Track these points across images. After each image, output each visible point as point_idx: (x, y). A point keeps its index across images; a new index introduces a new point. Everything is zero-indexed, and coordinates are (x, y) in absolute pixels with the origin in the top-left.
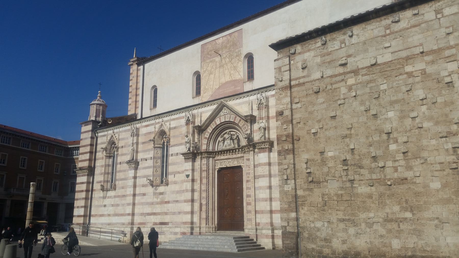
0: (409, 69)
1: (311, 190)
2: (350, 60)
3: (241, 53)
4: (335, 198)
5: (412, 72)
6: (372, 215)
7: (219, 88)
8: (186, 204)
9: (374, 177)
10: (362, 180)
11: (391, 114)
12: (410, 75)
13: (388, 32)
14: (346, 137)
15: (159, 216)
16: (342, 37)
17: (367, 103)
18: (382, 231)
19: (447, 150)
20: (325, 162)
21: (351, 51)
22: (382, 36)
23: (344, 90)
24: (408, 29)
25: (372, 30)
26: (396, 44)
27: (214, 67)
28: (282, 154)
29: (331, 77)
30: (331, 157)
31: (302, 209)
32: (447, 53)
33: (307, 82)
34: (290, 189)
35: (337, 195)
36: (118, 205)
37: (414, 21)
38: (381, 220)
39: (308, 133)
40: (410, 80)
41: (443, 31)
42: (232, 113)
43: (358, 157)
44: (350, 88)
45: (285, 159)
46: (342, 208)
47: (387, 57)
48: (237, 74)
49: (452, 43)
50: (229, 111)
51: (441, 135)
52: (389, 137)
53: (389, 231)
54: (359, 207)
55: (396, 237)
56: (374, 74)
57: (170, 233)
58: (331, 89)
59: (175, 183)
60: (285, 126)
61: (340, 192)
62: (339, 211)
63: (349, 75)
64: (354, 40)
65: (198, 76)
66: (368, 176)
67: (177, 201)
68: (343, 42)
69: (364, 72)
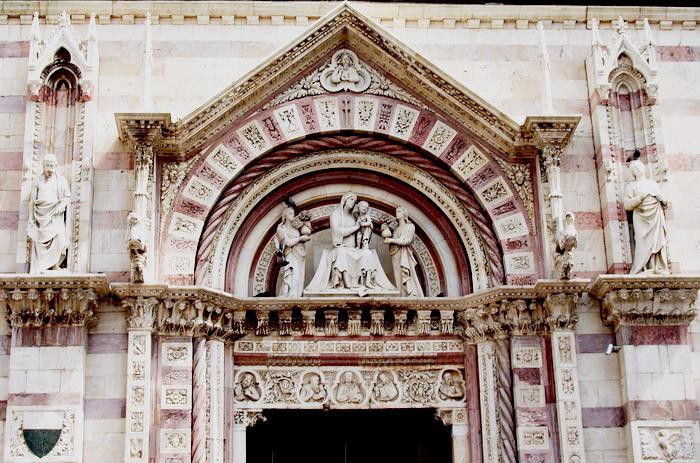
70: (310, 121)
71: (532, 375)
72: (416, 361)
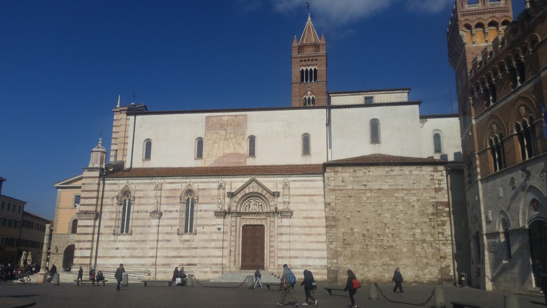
0: (396, 195)
1: (345, 248)
2: (368, 183)
3: (245, 133)
4: (358, 253)
5: (398, 197)
6: (376, 262)
7: (223, 156)
8: (217, 250)
9: (378, 244)
10: (372, 245)
11: (387, 215)
12: (397, 198)
13: (388, 174)
14: (365, 223)
15: (186, 259)
16: (364, 170)
17: (376, 208)
18: (381, 270)
19: (410, 235)
20: (353, 234)
21: (369, 179)
22: (385, 176)
23: (364, 198)
24: (397, 176)
25: (380, 171)
26: (391, 181)
27: (219, 138)
28: (329, 227)
29: (358, 190)
30: (357, 232)
31: (340, 258)
32: (413, 192)
33: (344, 189)
34: (334, 247)
35: (359, 251)
36: (135, 249)
37: (400, 173)
38: (380, 264)
39: (344, 218)
40: (397, 201)
41: (411, 182)
42: (259, 186)
43: (370, 234)
44: (368, 198)
45: (331, 230)
46: (362, 258)
47: (387, 187)
48: (241, 149)
49: (415, 188)
50: (257, 185)
51: (409, 228)
52: (386, 226)
53: (384, 270)
54: (370, 258)
55: (387, 272)
56: (380, 193)
57: (199, 272)
58: (358, 196)
59: (204, 233)
60: (331, 212)
61: (361, 250)
62: (360, 259)
63: (367, 191)
64: (371, 174)
65: (200, 143)
66: (375, 243)
67: (206, 248)
68: (365, 173)
69: (375, 191)
70: (249, 191)
71: (272, 222)
72: (261, 219)
